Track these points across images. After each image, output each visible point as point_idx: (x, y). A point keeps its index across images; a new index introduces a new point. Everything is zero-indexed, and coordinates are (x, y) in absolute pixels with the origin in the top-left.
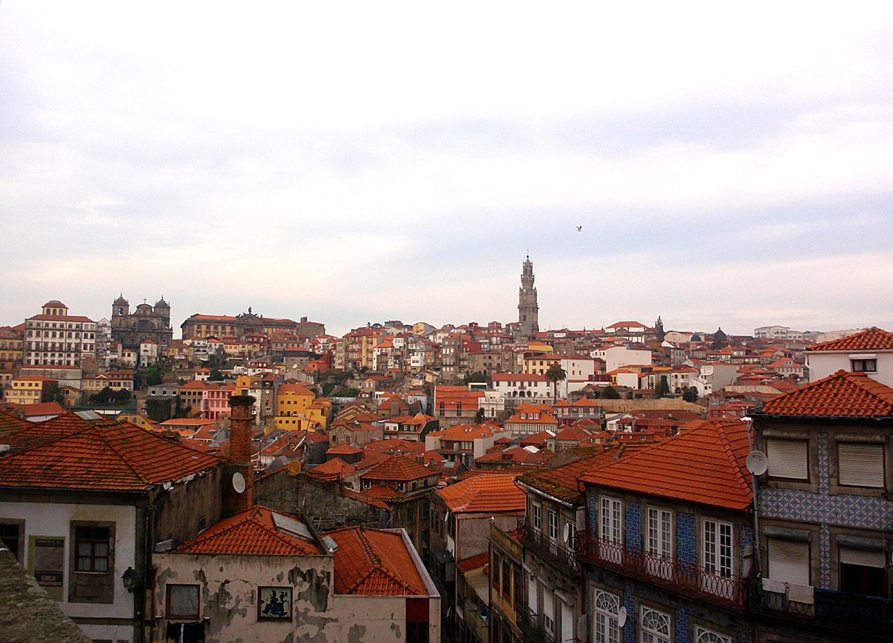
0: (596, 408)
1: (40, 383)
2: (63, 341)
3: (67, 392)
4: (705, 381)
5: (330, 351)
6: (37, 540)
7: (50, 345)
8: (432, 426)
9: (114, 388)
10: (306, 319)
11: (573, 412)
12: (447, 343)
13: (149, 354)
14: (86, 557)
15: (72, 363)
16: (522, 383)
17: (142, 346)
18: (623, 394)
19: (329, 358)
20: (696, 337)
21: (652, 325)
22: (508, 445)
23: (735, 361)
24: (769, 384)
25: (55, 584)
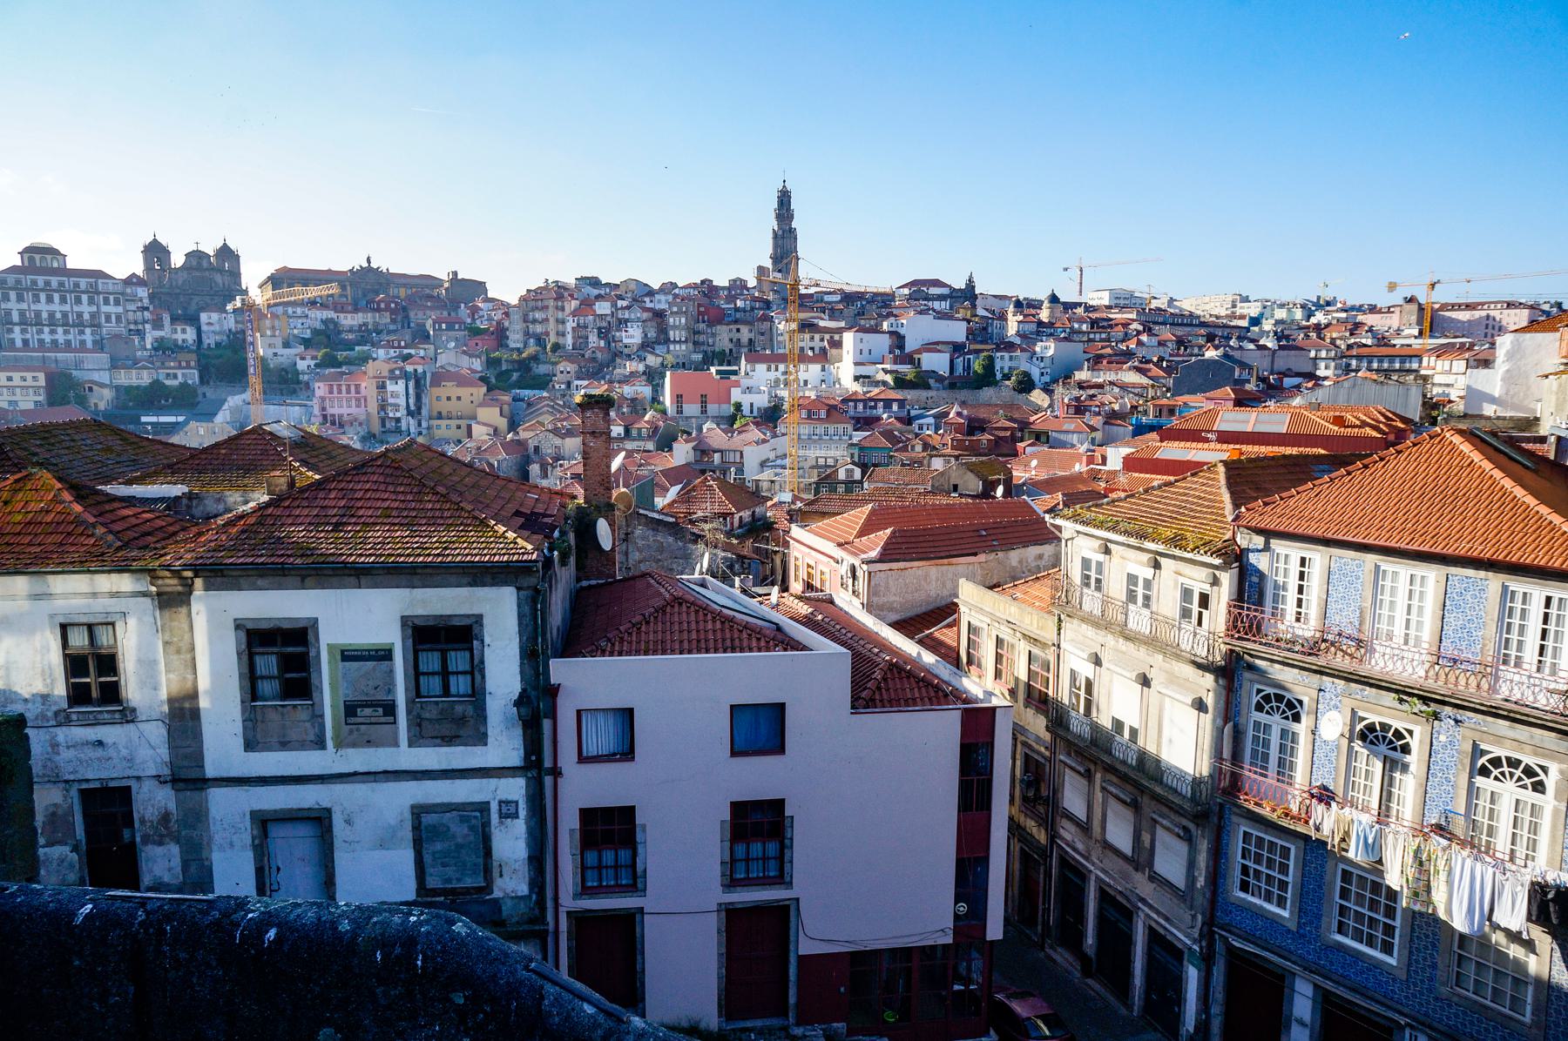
1: (41, 376)
2: (67, 308)
3: (91, 389)
5: (499, 323)
6: (343, 652)
7: (45, 315)
9: (168, 382)
10: (455, 273)
13: (217, 328)
14: (433, 674)
15: (89, 345)
17: (204, 317)
18: (932, 382)
19: (500, 334)
21: (960, 284)
23: (1075, 337)
25: (383, 720)
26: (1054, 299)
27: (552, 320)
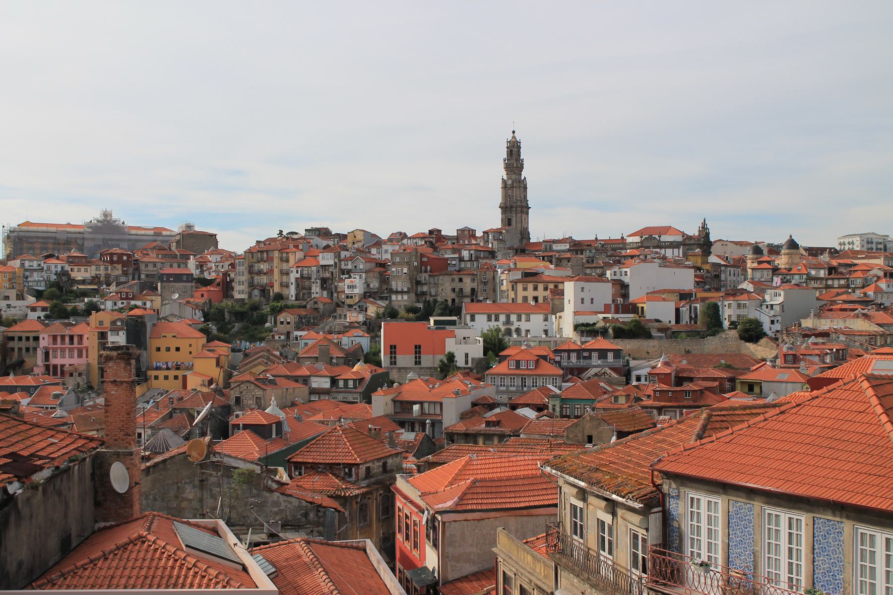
0: (617, 353)
4: (772, 313)
5: (226, 274)
8: (381, 381)
11: (585, 358)
12: (398, 260)
16: (508, 317)
18: (654, 333)
20: (757, 250)
21: (693, 230)
22: (492, 406)
23: (813, 284)
24: (866, 316)
26: (792, 245)
27: (276, 272)
